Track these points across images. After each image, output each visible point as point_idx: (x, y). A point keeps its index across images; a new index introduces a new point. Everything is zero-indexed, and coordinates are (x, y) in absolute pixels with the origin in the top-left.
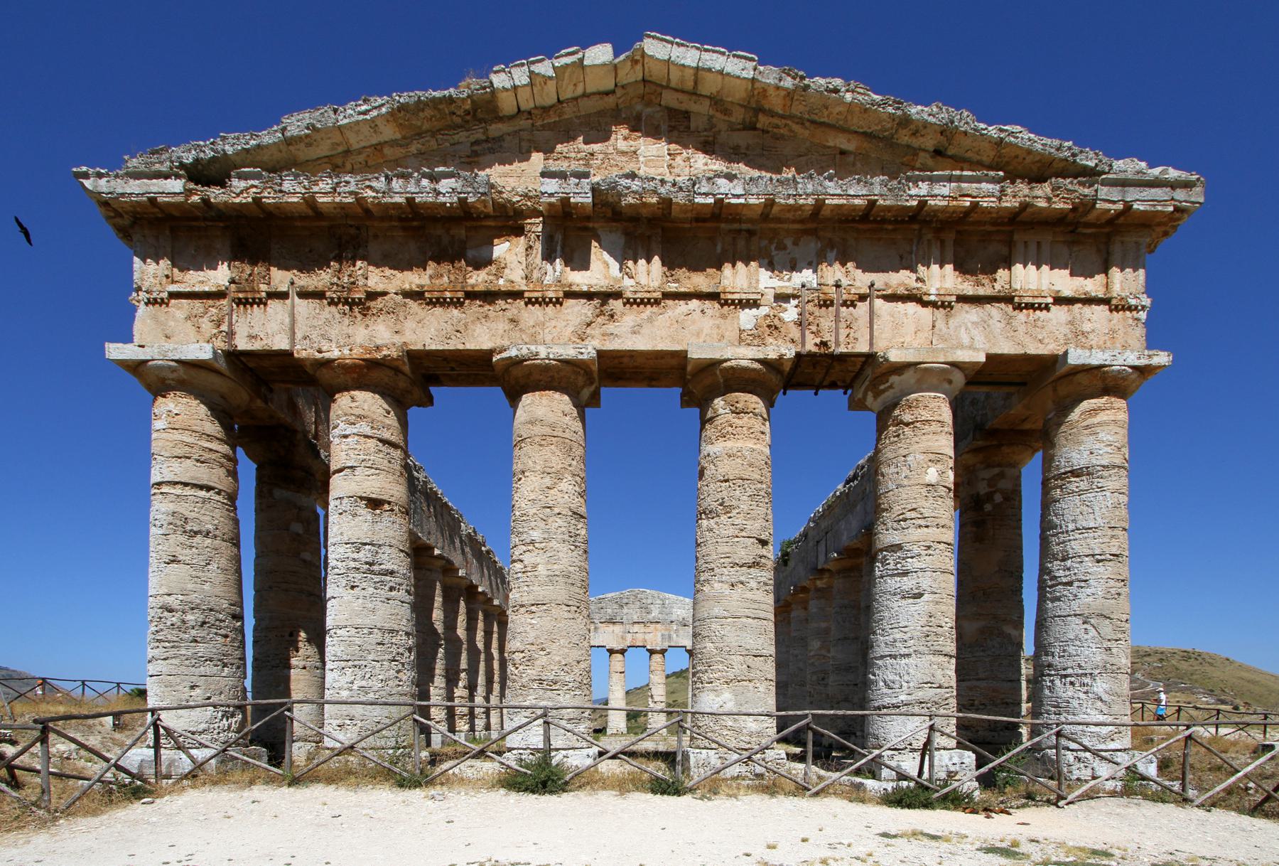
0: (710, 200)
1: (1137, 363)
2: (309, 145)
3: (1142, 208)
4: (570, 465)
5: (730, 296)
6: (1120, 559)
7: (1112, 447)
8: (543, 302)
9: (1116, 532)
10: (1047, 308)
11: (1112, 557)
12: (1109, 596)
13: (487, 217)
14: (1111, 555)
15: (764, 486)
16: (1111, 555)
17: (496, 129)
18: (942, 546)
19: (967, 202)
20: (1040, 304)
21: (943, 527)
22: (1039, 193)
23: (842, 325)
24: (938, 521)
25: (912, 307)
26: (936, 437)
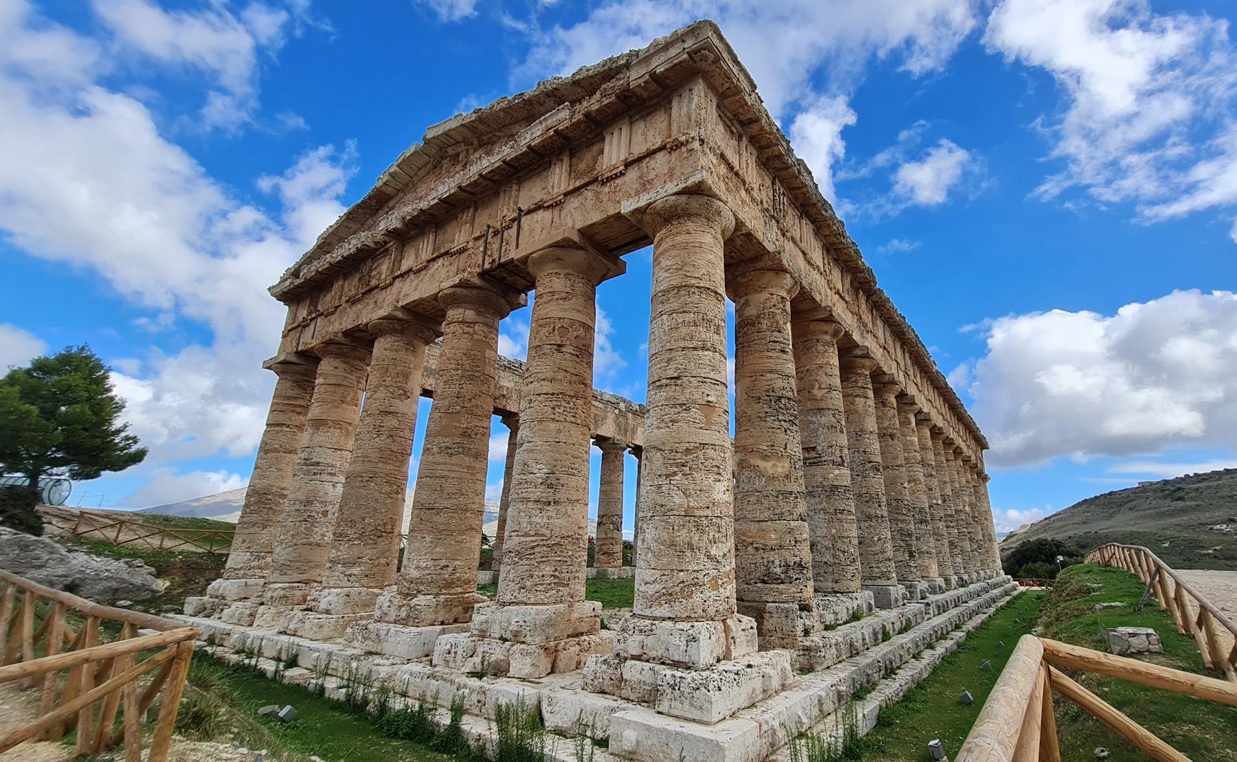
0: (436, 201)
1: (675, 190)
2: (328, 245)
3: (662, 70)
4: (384, 381)
5: (453, 251)
6: (679, 382)
7: (671, 271)
8: (386, 287)
9: (673, 354)
10: (622, 174)
11: (668, 381)
12: (663, 425)
13: (376, 250)
14: (667, 379)
15: (460, 372)
16: (667, 379)
17: (391, 204)
18: (541, 398)
19: (552, 132)
20: (616, 174)
21: (544, 380)
22: (592, 101)
23: (504, 243)
24: (540, 375)
25: (540, 212)
26: (546, 305)
